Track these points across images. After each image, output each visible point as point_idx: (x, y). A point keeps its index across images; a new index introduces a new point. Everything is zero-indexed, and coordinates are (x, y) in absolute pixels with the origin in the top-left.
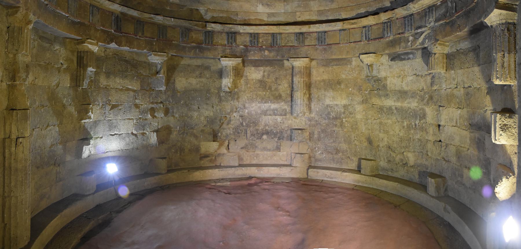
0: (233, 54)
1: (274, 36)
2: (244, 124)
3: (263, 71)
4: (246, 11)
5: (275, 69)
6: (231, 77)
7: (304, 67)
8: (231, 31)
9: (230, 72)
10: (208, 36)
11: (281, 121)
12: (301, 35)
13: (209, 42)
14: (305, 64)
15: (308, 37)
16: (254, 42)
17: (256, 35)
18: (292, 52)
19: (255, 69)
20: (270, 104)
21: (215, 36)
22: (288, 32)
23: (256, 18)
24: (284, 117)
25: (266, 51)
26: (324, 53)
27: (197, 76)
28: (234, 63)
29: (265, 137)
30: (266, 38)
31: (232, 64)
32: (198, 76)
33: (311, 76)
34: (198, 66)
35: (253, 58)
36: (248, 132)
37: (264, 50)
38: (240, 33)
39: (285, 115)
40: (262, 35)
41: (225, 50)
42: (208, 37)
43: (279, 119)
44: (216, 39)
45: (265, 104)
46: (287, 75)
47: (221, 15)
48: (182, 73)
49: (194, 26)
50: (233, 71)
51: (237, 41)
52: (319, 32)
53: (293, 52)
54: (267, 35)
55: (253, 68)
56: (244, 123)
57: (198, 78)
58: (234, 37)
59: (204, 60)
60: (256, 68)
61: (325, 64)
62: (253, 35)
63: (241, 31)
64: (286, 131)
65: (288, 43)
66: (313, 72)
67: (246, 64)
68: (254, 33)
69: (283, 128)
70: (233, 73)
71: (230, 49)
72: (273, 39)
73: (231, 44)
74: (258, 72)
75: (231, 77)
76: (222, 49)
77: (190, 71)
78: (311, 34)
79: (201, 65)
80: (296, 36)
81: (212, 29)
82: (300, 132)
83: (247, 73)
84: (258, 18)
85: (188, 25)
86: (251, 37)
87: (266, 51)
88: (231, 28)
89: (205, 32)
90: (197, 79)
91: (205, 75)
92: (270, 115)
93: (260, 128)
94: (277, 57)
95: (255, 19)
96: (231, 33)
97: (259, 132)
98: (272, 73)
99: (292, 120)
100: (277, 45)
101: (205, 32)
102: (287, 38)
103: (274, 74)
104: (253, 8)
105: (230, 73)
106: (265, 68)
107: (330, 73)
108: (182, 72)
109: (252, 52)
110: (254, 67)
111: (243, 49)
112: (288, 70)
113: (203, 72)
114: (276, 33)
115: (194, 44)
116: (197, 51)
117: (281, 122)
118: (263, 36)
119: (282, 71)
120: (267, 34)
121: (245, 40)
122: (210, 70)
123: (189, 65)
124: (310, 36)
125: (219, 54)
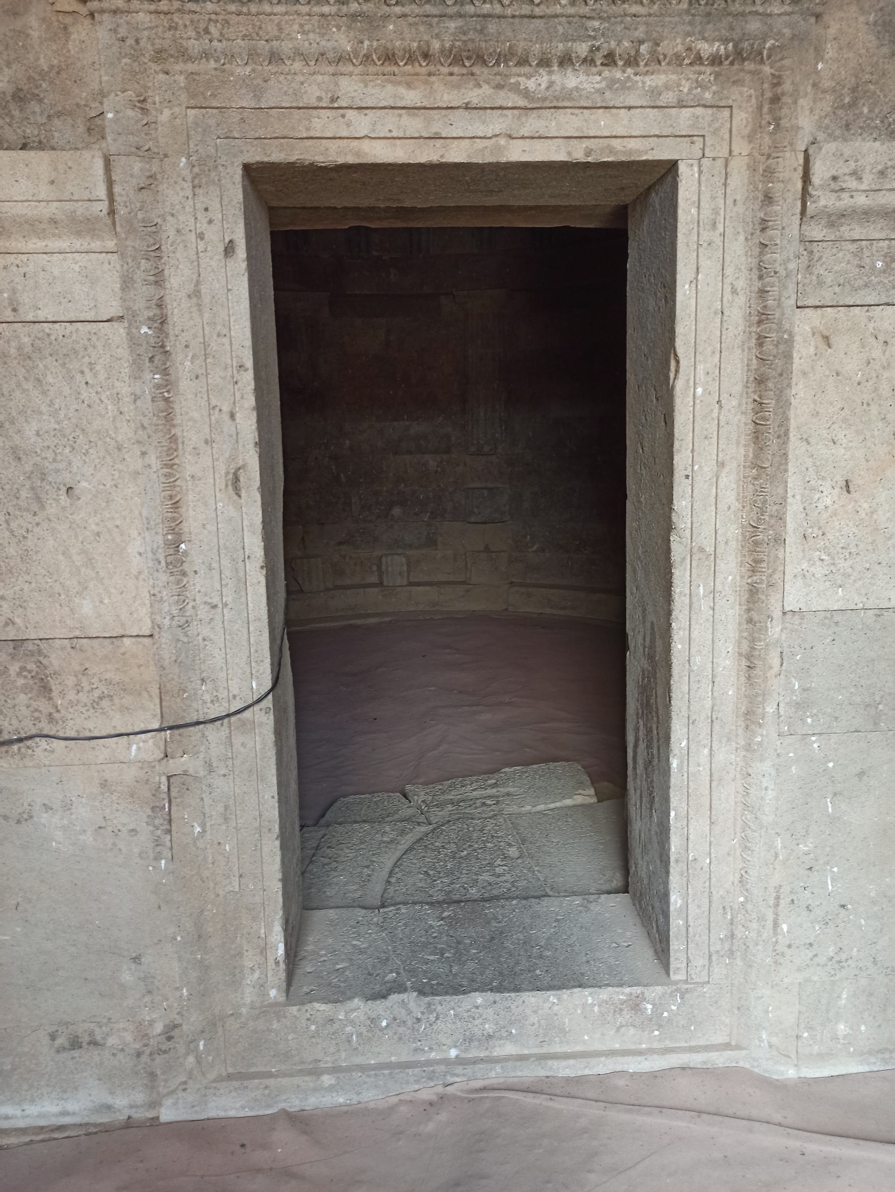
2: (343, 478)
11: (437, 466)
20: (407, 423)
24: (445, 457)
29: (397, 511)
36: (353, 501)
39: (448, 451)
43: (432, 462)
45: (395, 423)
56: (342, 476)
64: (450, 493)
69: (442, 486)
82: (486, 495)
92: (411, 453)
93: (385, 489)
97: (381, 499)
99: (465, 465)
117: (436, 472)
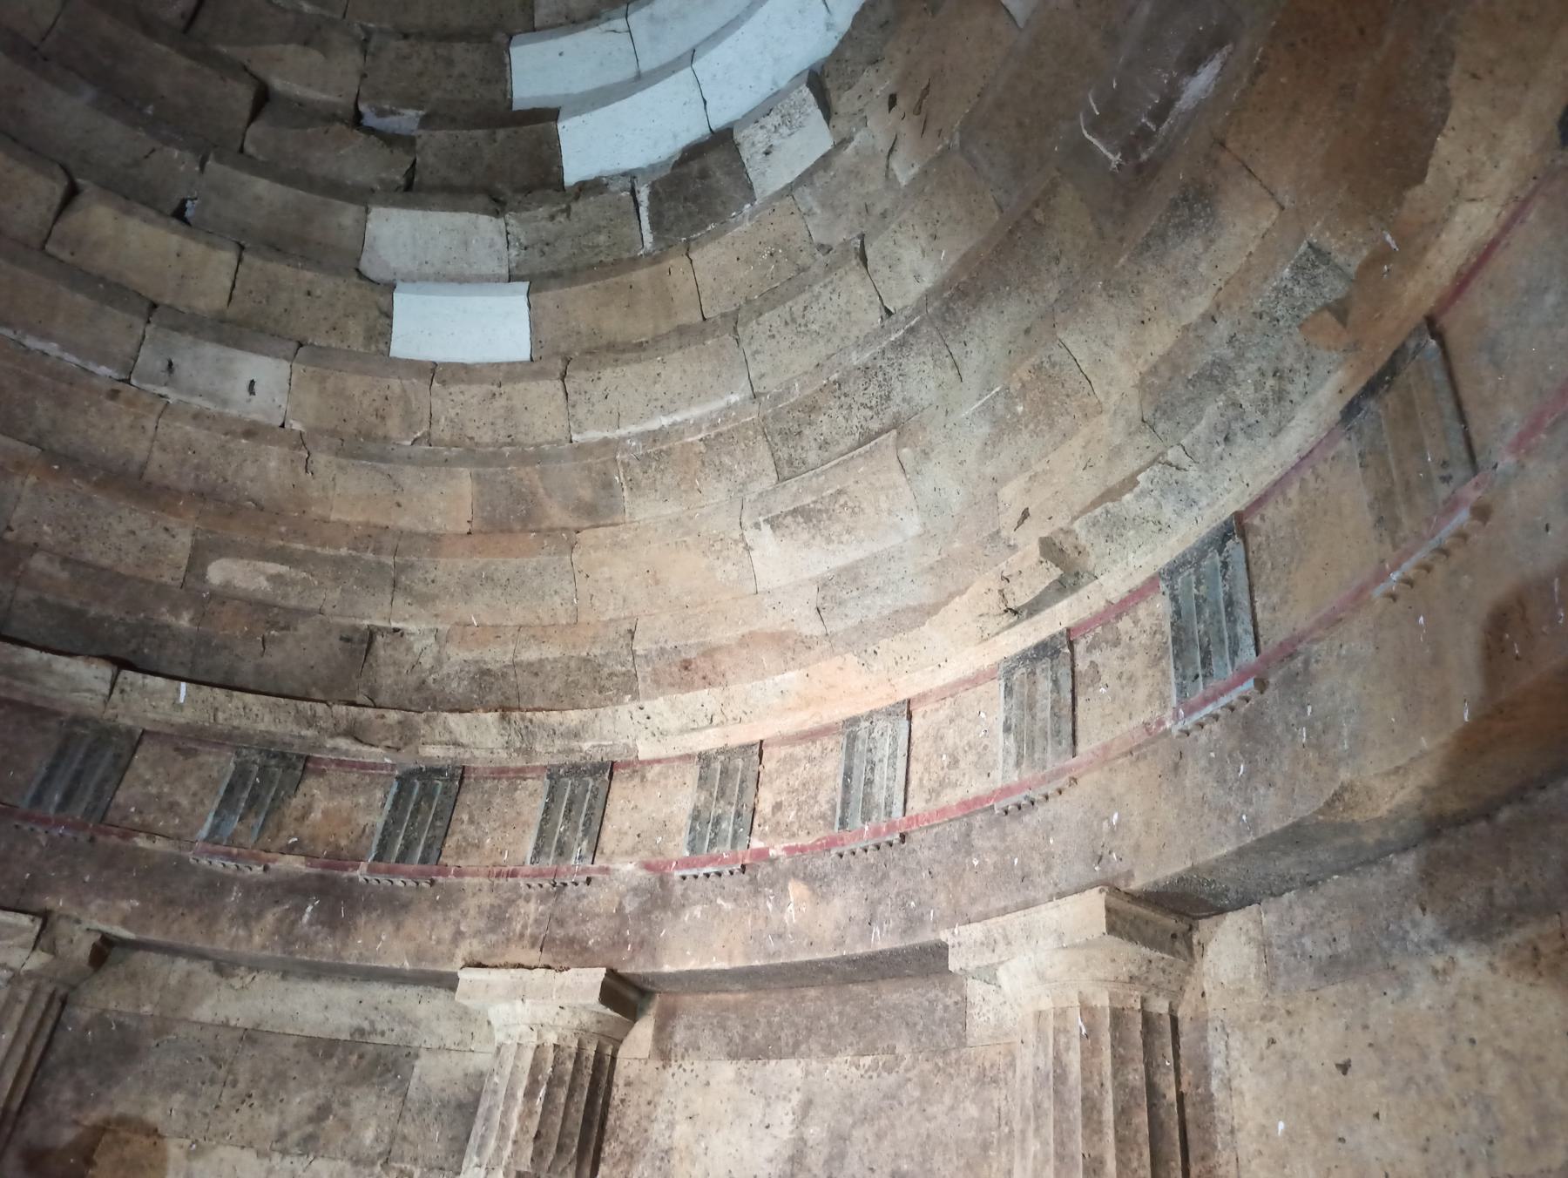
0: (560, 933)
1: (852, 739)
3: (796, 1098)
4: (687, 599)
5: (890, 1080)
6: (499, 1149)
7: (1087, 1010)
8: (576, 758)
9: (510, 1095)
10: (418, 804)
12: (1045, 663)
13: (408, 846)
14: (1100, 974)
15: (1107, 659)
16: (717, 821)
17: (740, 763)
18: (985, 853)
19: (739, 1079)
21: (466, 798)
22: (948, 675)
23: (744, 630)
25: (796, 889)
26: (1250, 775)
27: (282, 1135)
28: (545, 1011)
30: (802, 772)
31: (538, 1027)
32: (295, 1136)
33: (1220, 1139)
34: (323, 1048)
35: (692, 965)
37: (778, 883)
38: (637, 768)
40: (784, 751)
41: (511, 902)
42: (417, 810)
44: (471, 821)
46: (985, 1147)
47: (530, 654)
48: (178, 1099)
49: (332, 736)
50: (530, 1094)
51: (609, 827)
52: (1172, 571)
53: (990, 860)
54: (815, 751)
55: (726, 1071)
57: (284, 1153)
58: (588, 795)
59: (381, 993)
60: (749, 1068)
61: (1344, 945)
62: (718, 766)
63: (645, 751)
65: (954, 775)
66: (1227, 1084)
67: (680, 1035)
68: (722, 751)
70: (528, 1114)
71: (543, 899)
72: (848, 774)
73: (562, 850)
74: (756, 1111)
75: (499, 1149)
76: (487, 900)
77: (241, 1086)
78: (1125, 624)
79: (345, 1036)
80: (1009, 691)
81: (452, 752)
83: (671, 1125)
84: (757, 626)
85: (295, 730)
86: (703, 780)
87: (796, 889)
88: (576, 735)
89: (405, 781)
90: (276, 1157)
91: (348, 1127)
94: (865, 936)
95: (744, 642)
96: (575, 770)
98: (866, 1118)
100: (866, 817)
101: (405, 781)
102: (951, 736)
103: (879, 1137)
104: (729, 566)
105: (505, 1114)
106: (814, 1065)
107: (1436, 1066)
108: (176, 1087)
109: (697, 911)
110: (733, 1056)
111: (636, 891)
112: (994, 1081)
113: (346, 1104)
114: (870, 716)
115: (294, 864)
116: (306, 918)
118: (791, 761)
119: (948, 1100)
120: (811, 736)
121: (666, 810)
122: (405, 1080)
123: (251, 1037)
124: (1116, 643)
125: (458, 936)
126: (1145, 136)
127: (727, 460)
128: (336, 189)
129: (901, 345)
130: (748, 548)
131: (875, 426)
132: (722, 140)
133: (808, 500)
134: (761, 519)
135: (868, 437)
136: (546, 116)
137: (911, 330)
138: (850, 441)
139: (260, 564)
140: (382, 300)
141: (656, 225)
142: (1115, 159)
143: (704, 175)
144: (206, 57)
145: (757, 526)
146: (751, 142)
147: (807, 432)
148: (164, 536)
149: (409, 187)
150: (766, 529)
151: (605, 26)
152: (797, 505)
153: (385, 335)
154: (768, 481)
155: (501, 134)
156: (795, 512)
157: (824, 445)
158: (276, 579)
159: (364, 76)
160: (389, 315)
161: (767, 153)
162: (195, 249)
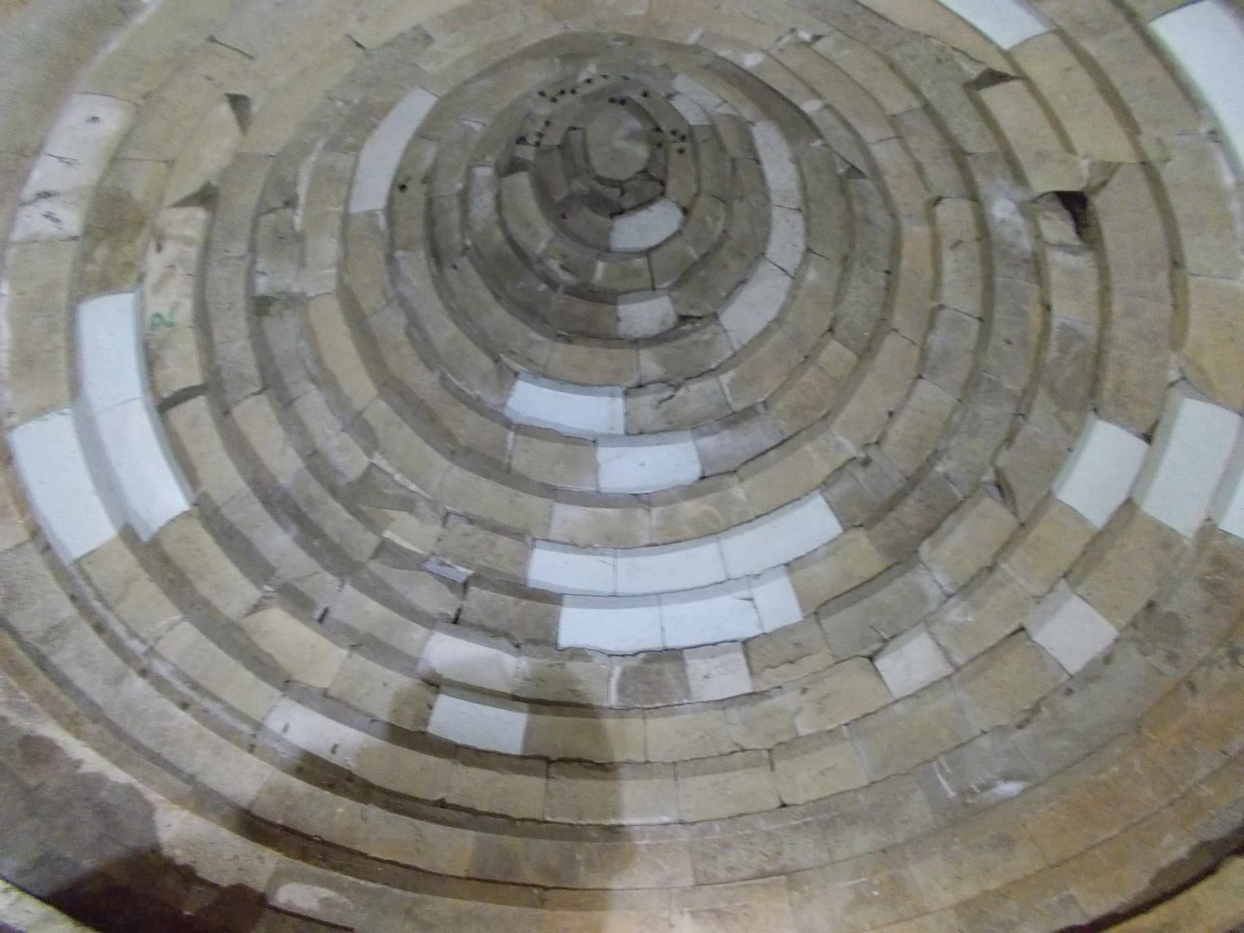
126: (972, 793)
127: (660, 862)
128: (413, 614)
129: (795, 828)
130: (672, 926)
131: (769, 868)
132: (674, 655)
133: (722, 905)
134: (686, 910)
135: (764, 874)
136: (552, 598)
137: (806, 824)
138: (747, 872)
139: (316, 889)
140: (431, 697)
141: (621, 690)
142: (952, 794)
143: (660, 673)
144: (356, 513)
145: (681, 913)
146: (697, 667)
147: (720, 858)
148: (256, 862)
149: (456, 621)
150: (687, 917)
151: (601, 558)
152: (715, 907)
153: (426, 722)
154: (688, 881)
155: (524, 602)
156: (711, 911)
157: (730, 869)
158: (325, 902)
159: (439, 540)
160: (431, 707)
161: (706, 677)
162: (323, 644)
